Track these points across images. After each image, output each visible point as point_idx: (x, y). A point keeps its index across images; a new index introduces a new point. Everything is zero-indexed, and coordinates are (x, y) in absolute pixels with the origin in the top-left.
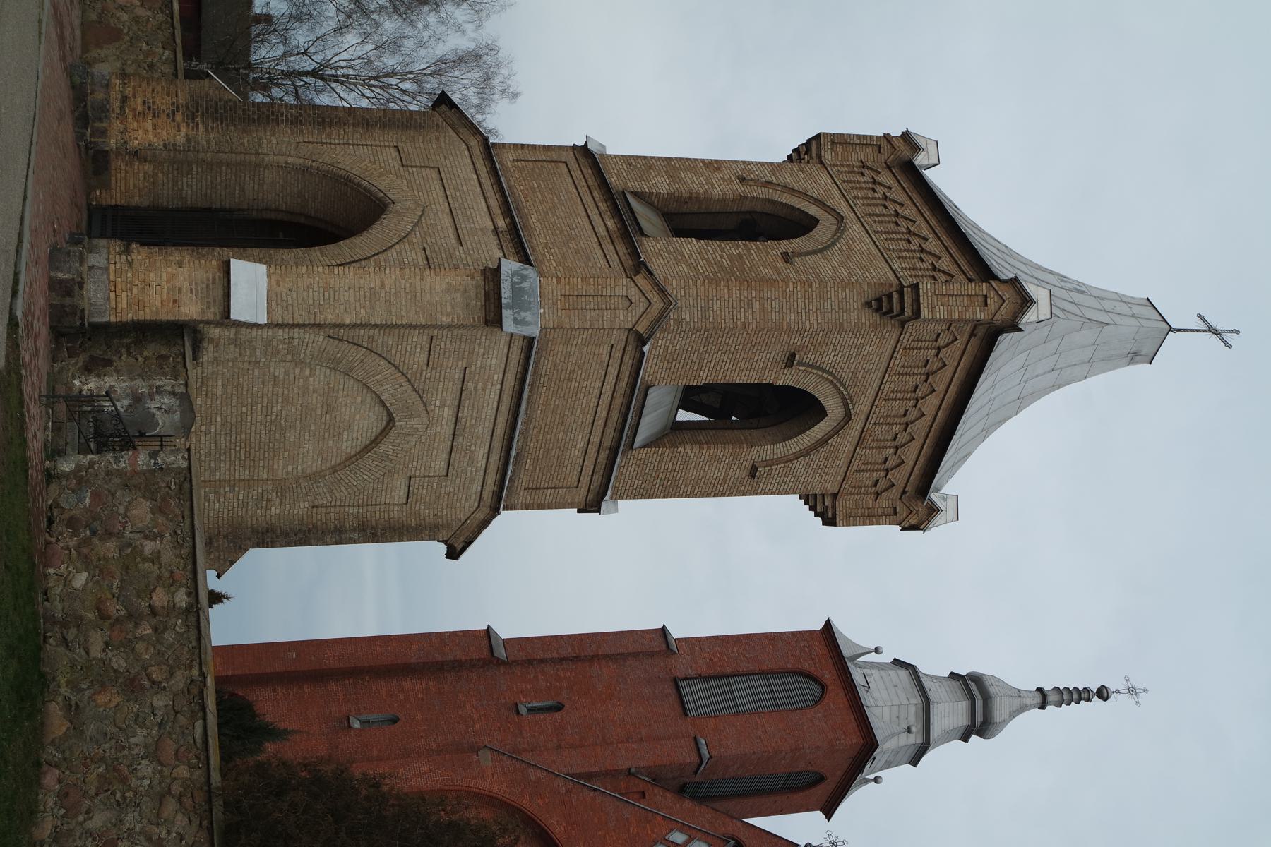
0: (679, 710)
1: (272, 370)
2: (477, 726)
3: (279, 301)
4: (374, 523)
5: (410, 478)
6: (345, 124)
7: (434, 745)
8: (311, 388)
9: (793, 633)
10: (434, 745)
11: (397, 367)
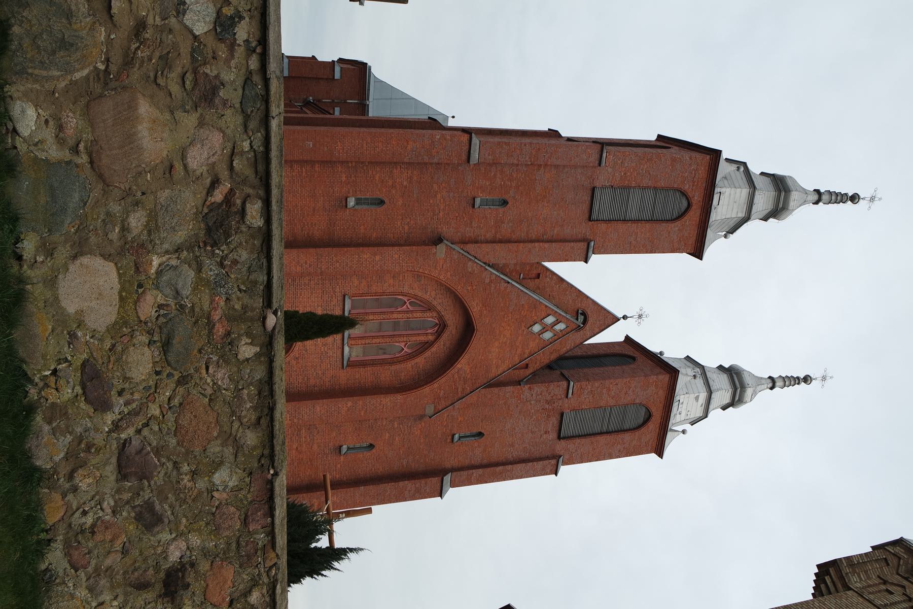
0: (587, 216)
2: (441, 214)
7: (406, 227)
10: (406, 227)
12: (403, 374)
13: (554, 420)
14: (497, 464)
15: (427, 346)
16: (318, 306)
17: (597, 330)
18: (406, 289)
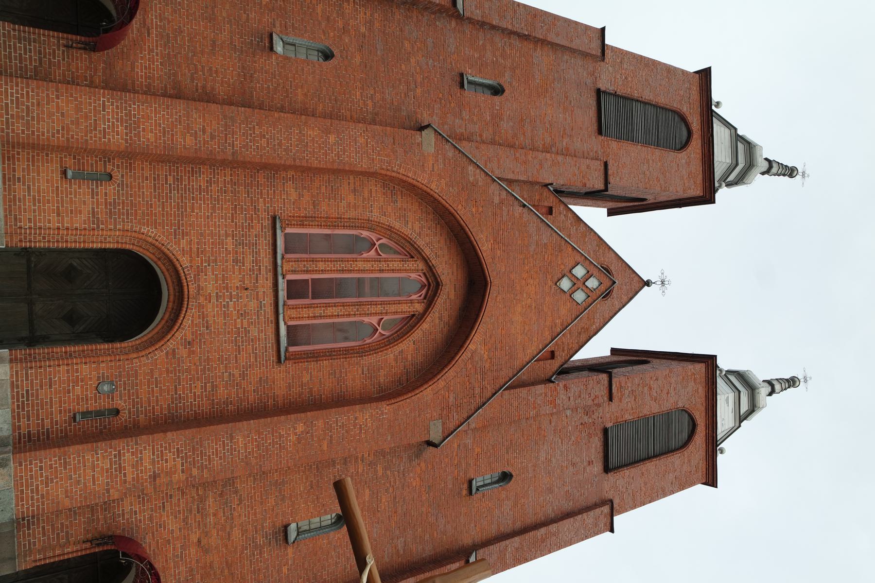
2: (419, 91)
9: (683, 71)
10: (369, 102)
12: (382, 373)
13: (597, 442)
14: (535, 526)
15: (412, 321)
16: (227, 235)
17: (625, 298)
18: (375, 215)
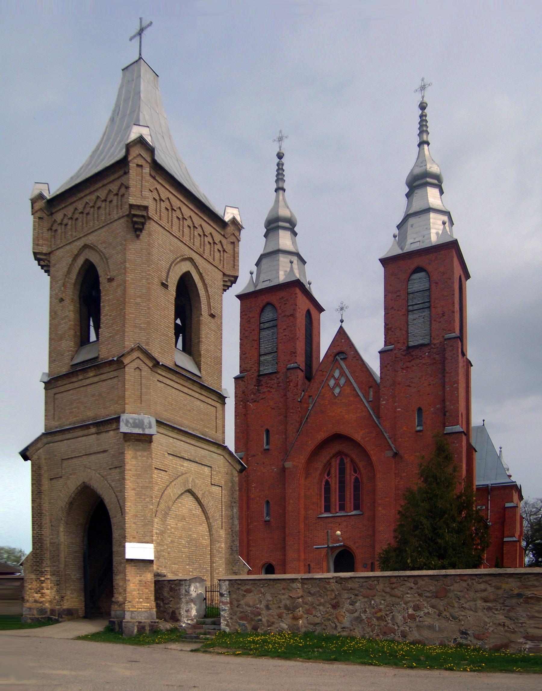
1: (168, 543)
3: (142, 538)
4: (230, 502)
5: (212, 484)
6: (40, 503)
8: (175, 526)
11: (168, 486)
